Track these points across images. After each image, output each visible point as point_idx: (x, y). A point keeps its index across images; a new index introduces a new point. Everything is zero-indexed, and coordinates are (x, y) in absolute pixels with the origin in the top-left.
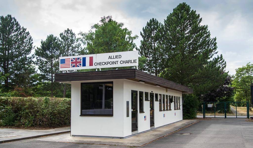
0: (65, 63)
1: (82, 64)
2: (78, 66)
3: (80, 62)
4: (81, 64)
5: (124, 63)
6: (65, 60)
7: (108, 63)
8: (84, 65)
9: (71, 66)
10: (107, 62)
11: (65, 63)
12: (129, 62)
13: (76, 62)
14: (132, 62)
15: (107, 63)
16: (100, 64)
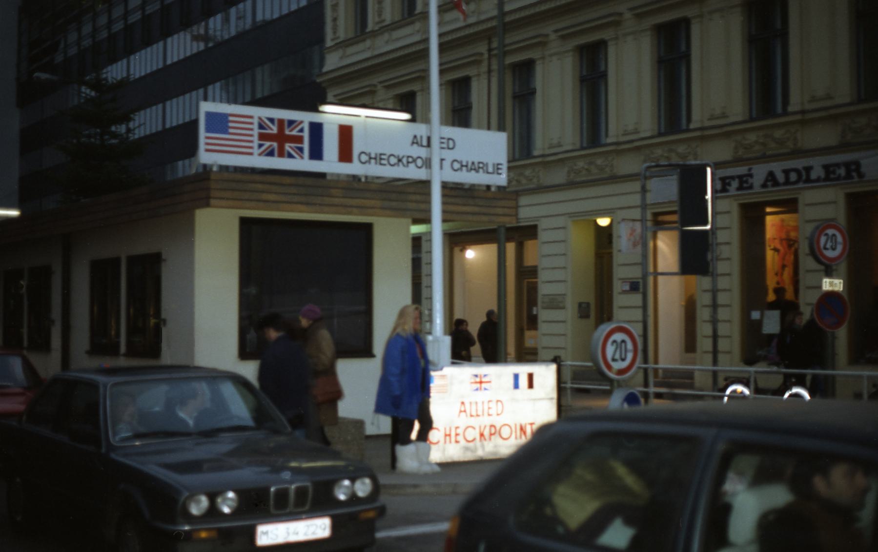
0: (231, 131)
1: (306, 146)
2: (290, 156)
3: (299, 139)
4: (301, 150)
5: (464, 168)
6: (231, 118)
7: (408, 162)
8: (317, 153)
9: (256, 151)
10: (408, 157)
11: (226, 132)
12: (481, 170)
13: (281, 138)
14: (490, 170)
15: (405, 160)
16: (379, 159)
